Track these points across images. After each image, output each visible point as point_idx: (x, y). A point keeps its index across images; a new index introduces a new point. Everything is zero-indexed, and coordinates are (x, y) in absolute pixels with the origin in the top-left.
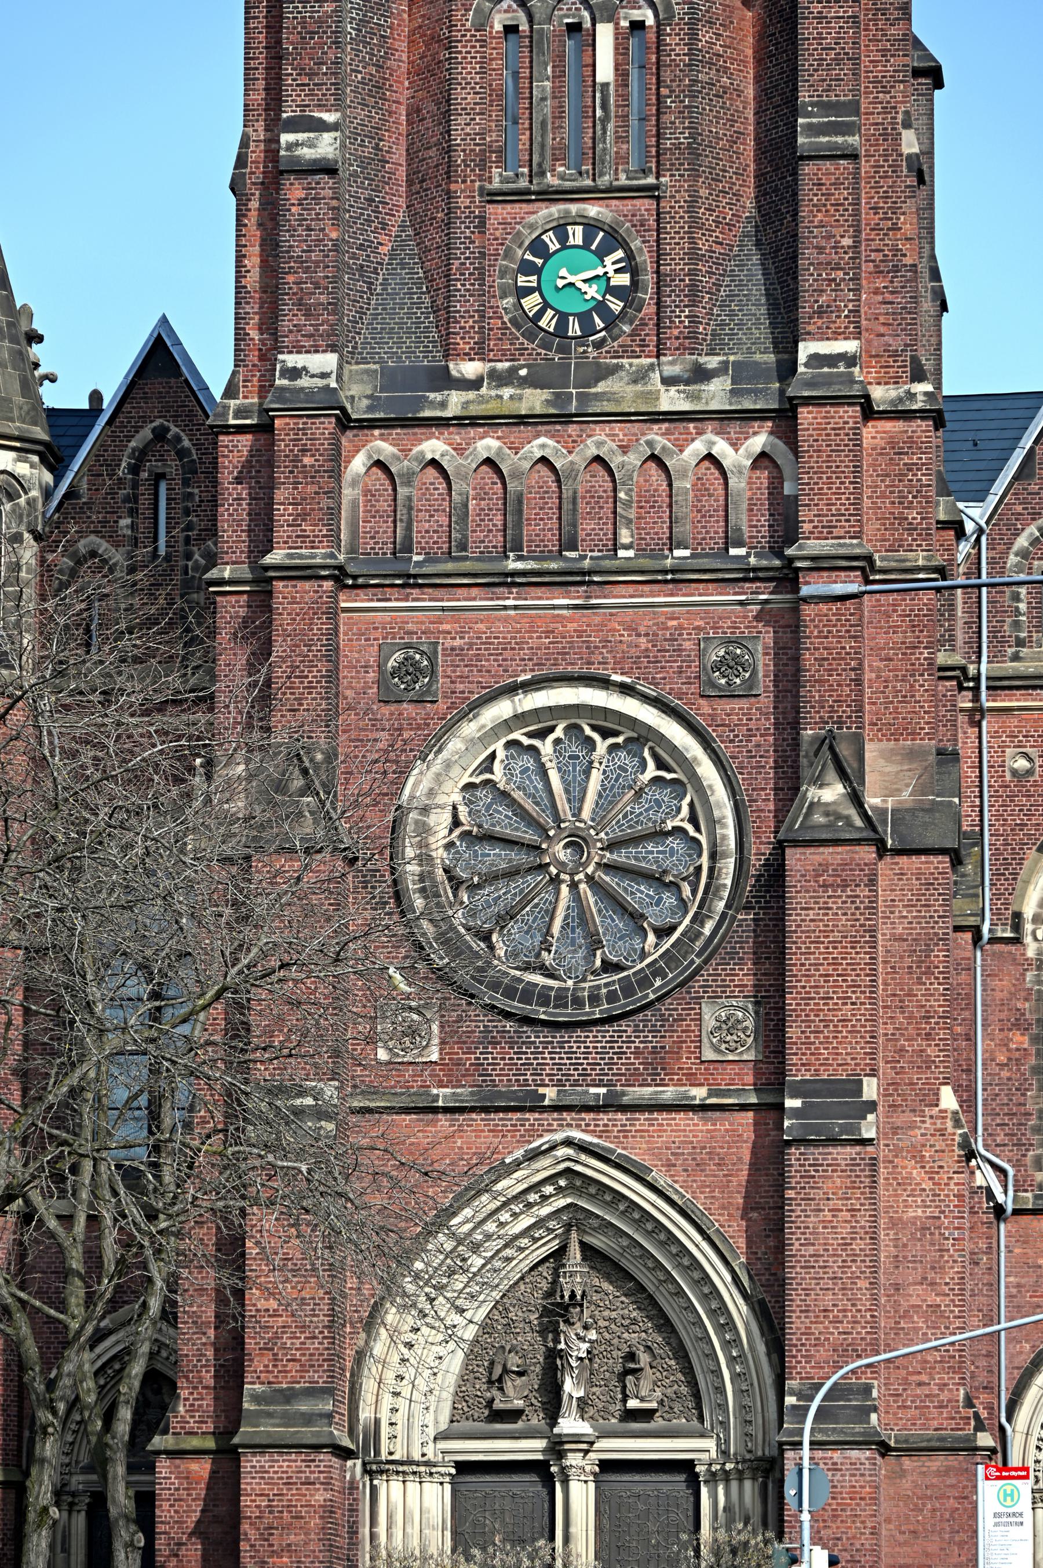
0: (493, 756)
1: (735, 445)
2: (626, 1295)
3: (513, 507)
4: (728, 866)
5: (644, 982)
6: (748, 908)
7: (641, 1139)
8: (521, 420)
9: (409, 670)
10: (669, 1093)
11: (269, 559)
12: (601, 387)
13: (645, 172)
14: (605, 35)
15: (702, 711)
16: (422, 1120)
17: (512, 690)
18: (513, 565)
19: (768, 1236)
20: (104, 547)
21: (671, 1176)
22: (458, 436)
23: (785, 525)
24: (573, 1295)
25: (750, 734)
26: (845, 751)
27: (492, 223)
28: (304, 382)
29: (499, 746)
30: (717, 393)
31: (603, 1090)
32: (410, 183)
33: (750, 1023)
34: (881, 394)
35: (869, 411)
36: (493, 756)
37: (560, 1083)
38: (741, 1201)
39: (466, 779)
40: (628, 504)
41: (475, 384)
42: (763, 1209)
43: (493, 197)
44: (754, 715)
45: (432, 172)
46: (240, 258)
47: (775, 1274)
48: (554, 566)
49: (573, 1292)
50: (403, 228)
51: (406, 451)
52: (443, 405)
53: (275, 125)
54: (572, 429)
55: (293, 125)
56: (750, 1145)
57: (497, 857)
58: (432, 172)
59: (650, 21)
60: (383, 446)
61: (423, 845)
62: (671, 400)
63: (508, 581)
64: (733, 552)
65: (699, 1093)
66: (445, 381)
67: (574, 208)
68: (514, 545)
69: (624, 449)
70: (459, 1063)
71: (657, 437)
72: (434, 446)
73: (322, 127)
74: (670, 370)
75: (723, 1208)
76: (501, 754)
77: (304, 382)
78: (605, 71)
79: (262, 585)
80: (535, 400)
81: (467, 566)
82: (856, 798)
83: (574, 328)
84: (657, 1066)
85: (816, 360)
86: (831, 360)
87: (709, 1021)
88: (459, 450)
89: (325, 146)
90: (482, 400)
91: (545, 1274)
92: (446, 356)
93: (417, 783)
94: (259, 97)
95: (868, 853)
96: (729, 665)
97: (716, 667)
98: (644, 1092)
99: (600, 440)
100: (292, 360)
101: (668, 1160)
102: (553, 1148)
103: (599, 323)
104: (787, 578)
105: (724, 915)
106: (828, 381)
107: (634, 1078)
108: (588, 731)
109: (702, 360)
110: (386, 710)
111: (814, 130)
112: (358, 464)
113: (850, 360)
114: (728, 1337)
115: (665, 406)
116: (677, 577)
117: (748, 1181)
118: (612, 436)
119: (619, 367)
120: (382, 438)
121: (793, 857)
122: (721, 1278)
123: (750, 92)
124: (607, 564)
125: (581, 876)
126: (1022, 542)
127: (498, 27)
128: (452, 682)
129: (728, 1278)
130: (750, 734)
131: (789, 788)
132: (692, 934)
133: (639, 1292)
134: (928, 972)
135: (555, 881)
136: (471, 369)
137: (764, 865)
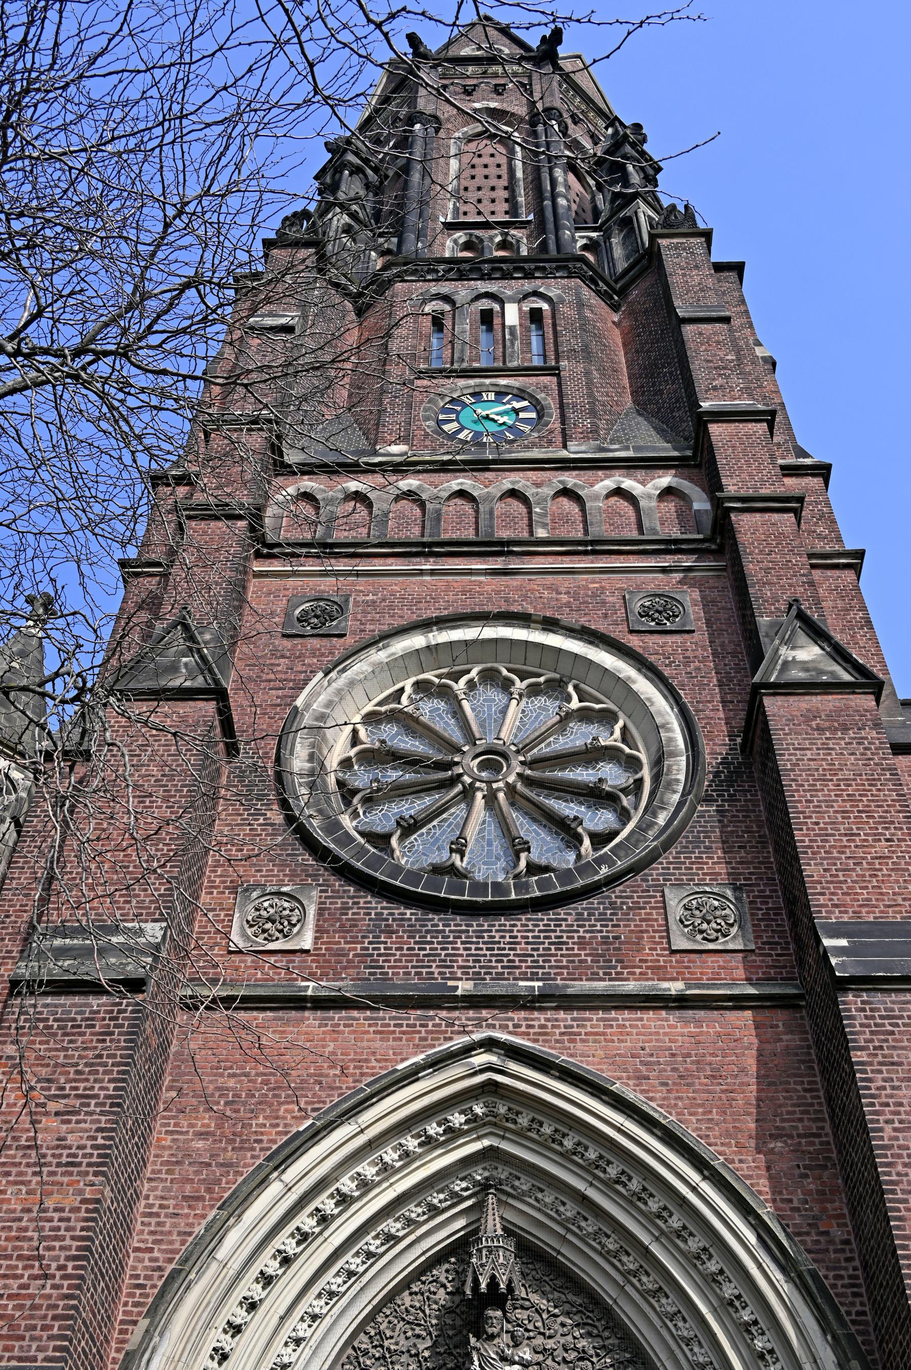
0: (402, 690)
2: (567, 1314)
4: (679, 767)
6: (708, 800)
7: (592, 1041)
16: (281, 1019)
19: (806, 1176)
21: (642, 1092)
24: (493, 1282)
25: (687, 661)
31: (540, 984)
33: (730, 912)
36: (402, 690)
37: (477, 977)
38: (753, 1125)
39: (370, 707)
42: (791, 1137)
47: (827, 1233)
49: (493, 1277)
56: (754, 1052)
70: (342, 954)
75: (728, 1135)
76: (408, 690)
87: (676, 910)
91: (443, 1279)
93: (315, 696)
101: (637, 1070)
108: (505, 672)
114: (759, 1344)
117: (758, 1099)
120: (309, 480)
122: (740, 1237)
125: (501, 784)
128: (362, 624)
129: (751, 1238)
130: (687, 661)
133: (593, 1310)
137: (721, 763)
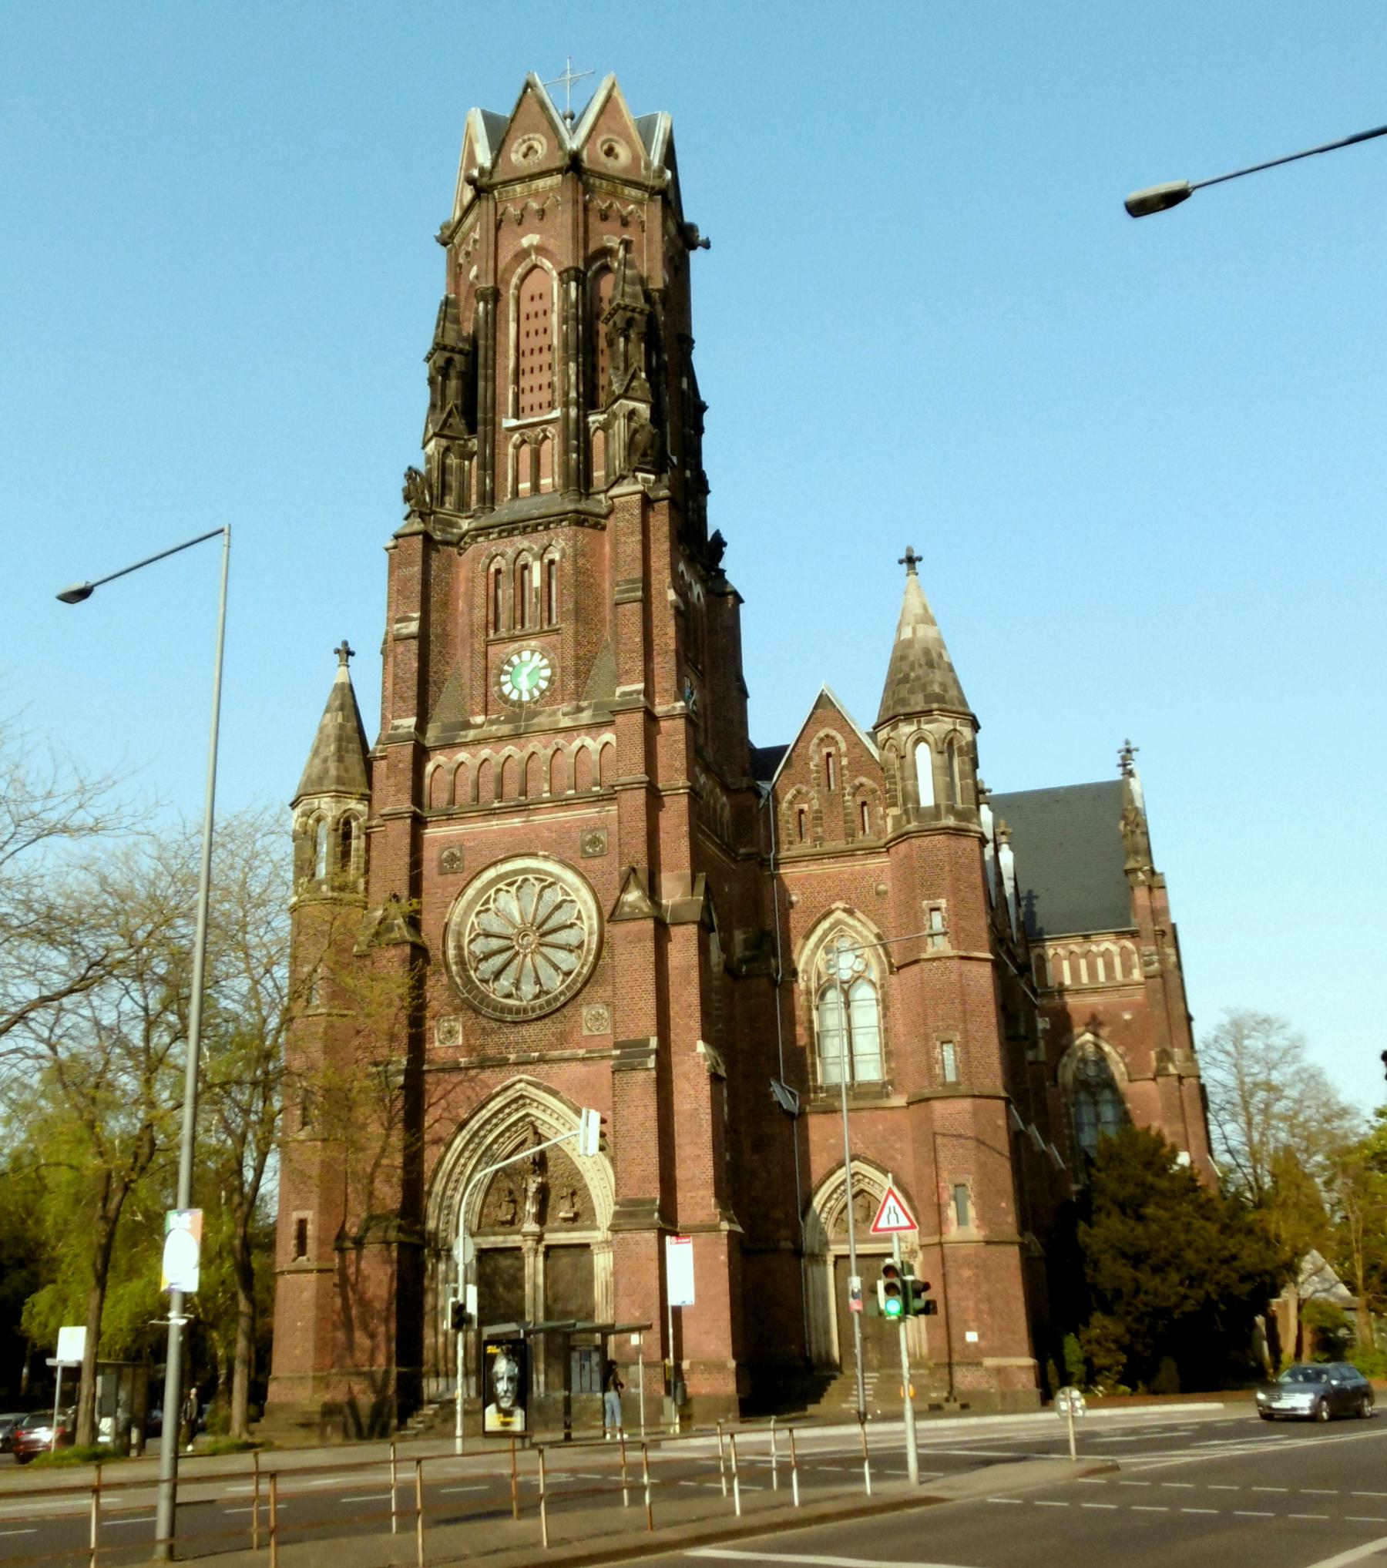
1: (594, 740)
5: (556, 999)
8: (500, 739)
9: (453, 858)
10: (567, 1053)
12: (535, 721)
15: (582, 864)
17: (495, 864)
22: (473, 749)
28: (400, 731)
30: (586, 717)
41: (481, 726)
46: (384, 683)
51: (450, 759)
54: (522, 741)
64: (595, 789)
65: (581, 1052)
66: (467, 725)
67: (525, 643)
69: (545, 747)
71: (560, 740)
77: (400, 731)
80: (506, 729)
84: (563, 1039)
85: (624, 694)
86: (630, 693)
88: (474, 756)
98: (556, 1053)
102: (514, 1084)
106: (628, 702)
107: (552, 1047)
115: (562, 725)
134: (689, 983)
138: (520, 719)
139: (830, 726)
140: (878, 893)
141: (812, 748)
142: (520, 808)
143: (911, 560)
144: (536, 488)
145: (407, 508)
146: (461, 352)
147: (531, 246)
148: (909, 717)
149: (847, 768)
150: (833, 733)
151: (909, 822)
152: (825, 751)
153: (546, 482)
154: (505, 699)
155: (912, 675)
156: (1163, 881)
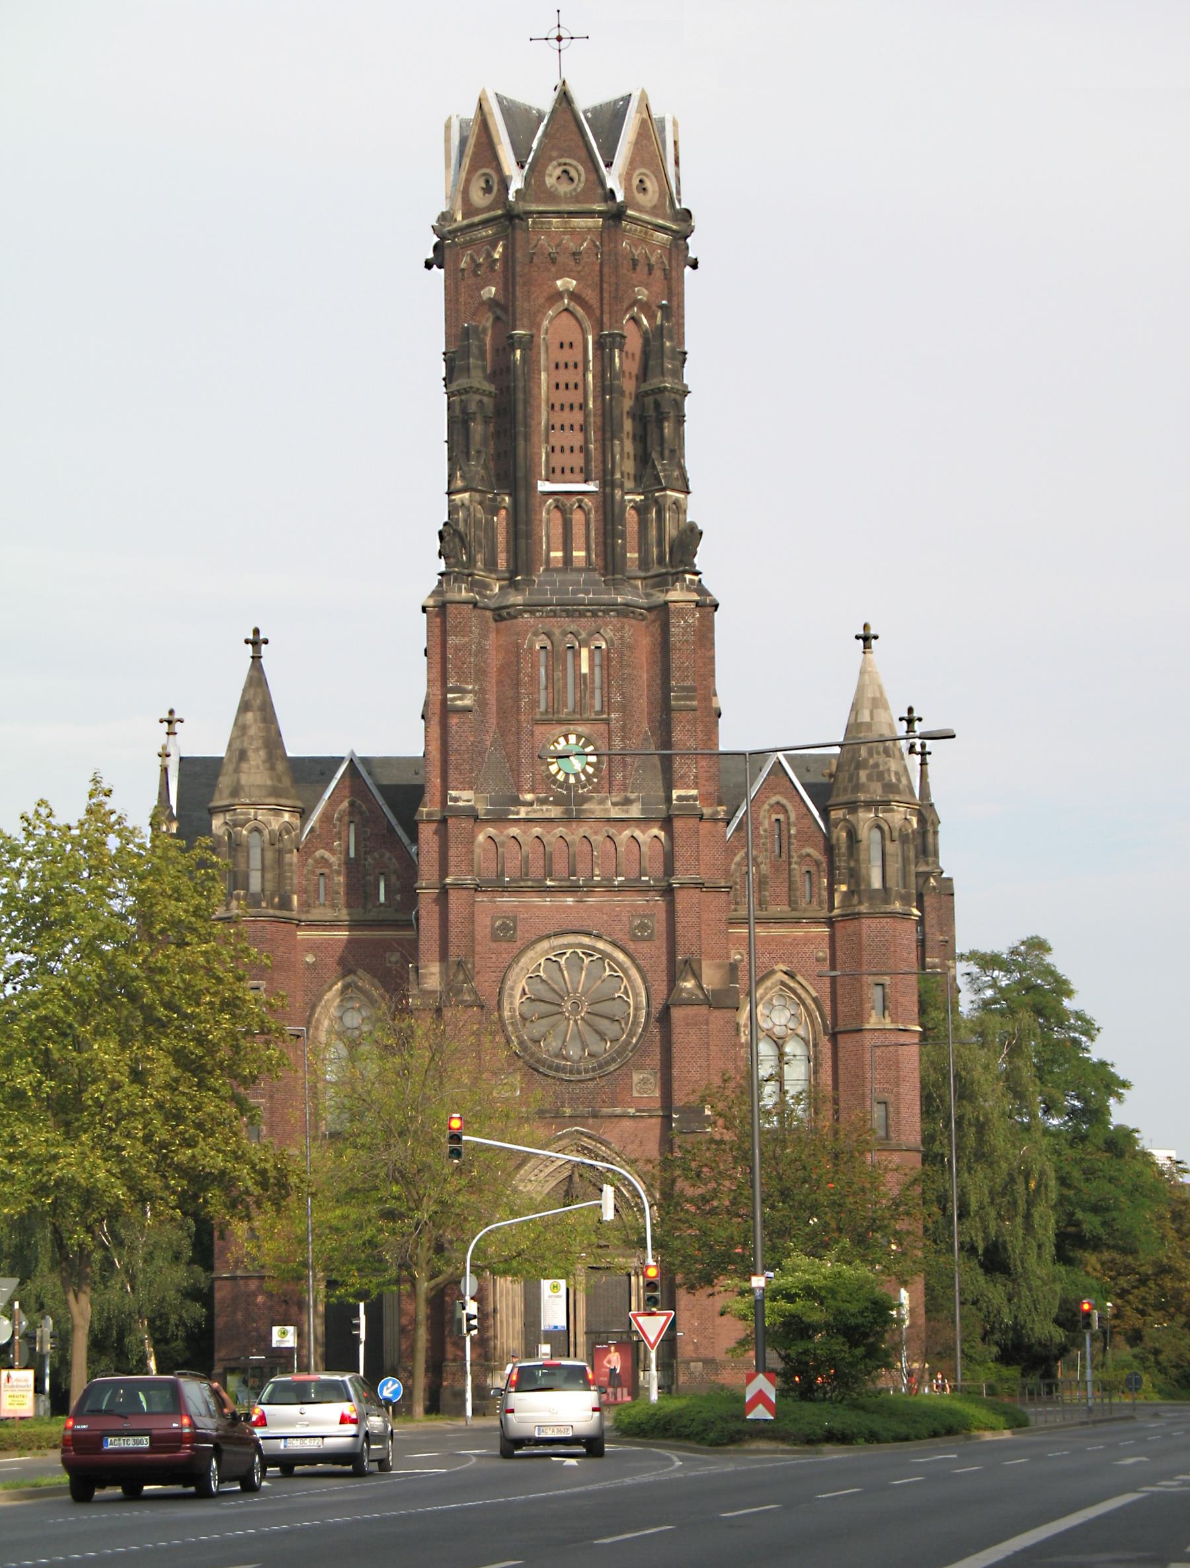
1: (643, 832)
3: (548, 858)
8: (551, 820)
10: (618, 1110)
11: (448, 880)
12: (585, 807)
13: (602, 712)
14: (584, 653)
15: (631, 946)
18: (549, 883)
20: (327, 855)
22: (523, 826)
23: (669, 870)
26: (695, 966)
27: (537, 733)
29: (542, 961)
30: (635, 811)
32: (498, 713)
34: (707, 811)
35: (701, 818)
40: (597, 857)
41: (531, 804)
43: (537, 722)
44: (655, 951)
45: (509, 711)
48: (563, 884)
50: (495, 733)
52: (518, 813)
53: (445, 690)
54: (574, 825)
55: (453, 691)
57: (543, 1008)
58: (509, 711)
59: (604, 647)
60: (491, 831)
61: (511, 1003)
62: (615, 813)
63: (549, 890)
65: (632, 1111)
67: (572, 727)
68: (549, 874)
69: (596, 833)
72: (514, 831)
73: (464, 692)
74: (614, 800)
77: (461, 804)
78: (585, 669)
79: (444, 890)
80: (554, 812)
81: (530, 883)
82: (701, 987)
83: (572, 780)
85: (680, 798)
88: (524, 832)
89: (468, 701)
90: (535, 811)
92: (518, 790)
94: (436, 675)
95: (704, 1010)
96: (642, 927)
97: (637, 927)
98: (606, 1111)
99: (584, 830)
100: (453, 793)
103: (583, 778)
104: (668, 892)
105: (641, 1035)
109: (629, 794)
110: (494, 945)
111: (677, 698)
112: (481, 838)
113: (695, 798)
116: (621, 889)
118: (591, 828)
119: (592, 797)
121: (677, 1014)
123: (645, 676)
124: (591, 884)
126: (737, 859)
127: (538, 647)
131: (673, 981)
132: (627, 1042)
135: (568, 1019)
136: (529, 797)
138: (570, 800)
139: (779, 793)
140: (817, 960)
141: (762, 813)
142: (573, 889)
143: (867, 639)
144: (568, 559)
145: (442, 565)
146: (490, 394)
147: (567, 291)
148: (869, 805)
149: (796, 837)
150: (784, 801)
151: (860, 903)
152: (774, 817)
153: (579, 554)
154: (552, 778)
155: (871, 762)
156: (951, 887)
